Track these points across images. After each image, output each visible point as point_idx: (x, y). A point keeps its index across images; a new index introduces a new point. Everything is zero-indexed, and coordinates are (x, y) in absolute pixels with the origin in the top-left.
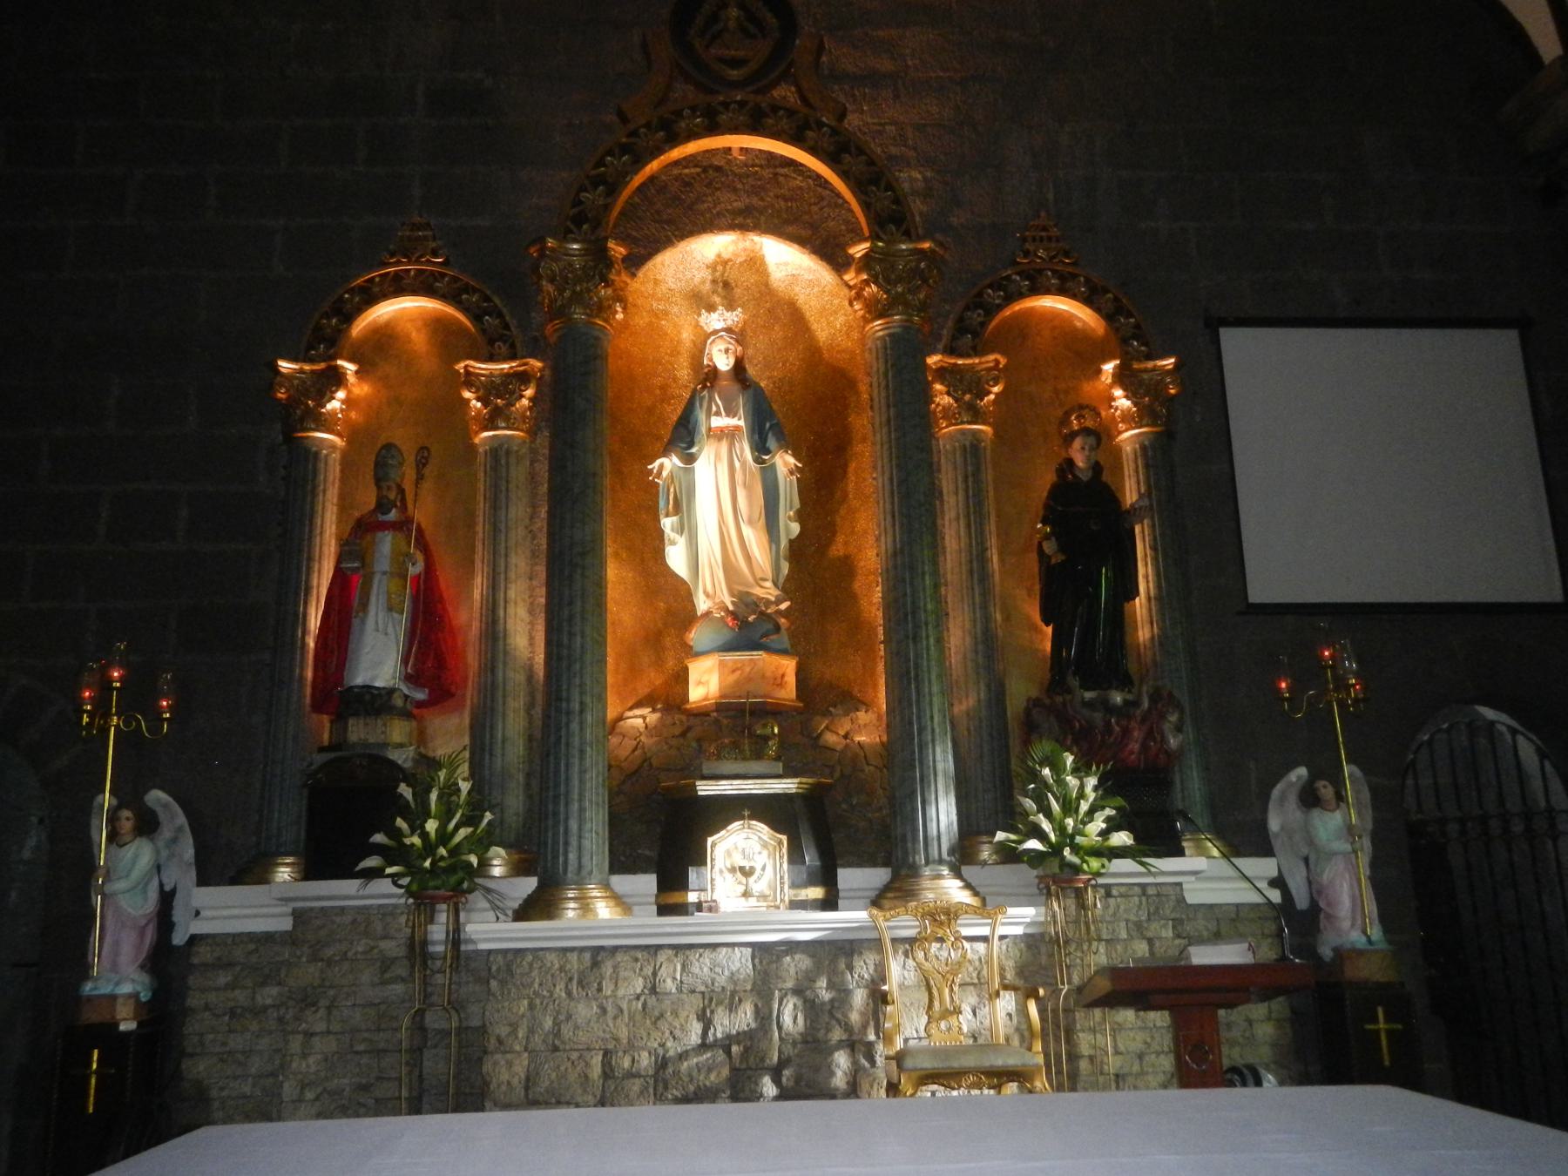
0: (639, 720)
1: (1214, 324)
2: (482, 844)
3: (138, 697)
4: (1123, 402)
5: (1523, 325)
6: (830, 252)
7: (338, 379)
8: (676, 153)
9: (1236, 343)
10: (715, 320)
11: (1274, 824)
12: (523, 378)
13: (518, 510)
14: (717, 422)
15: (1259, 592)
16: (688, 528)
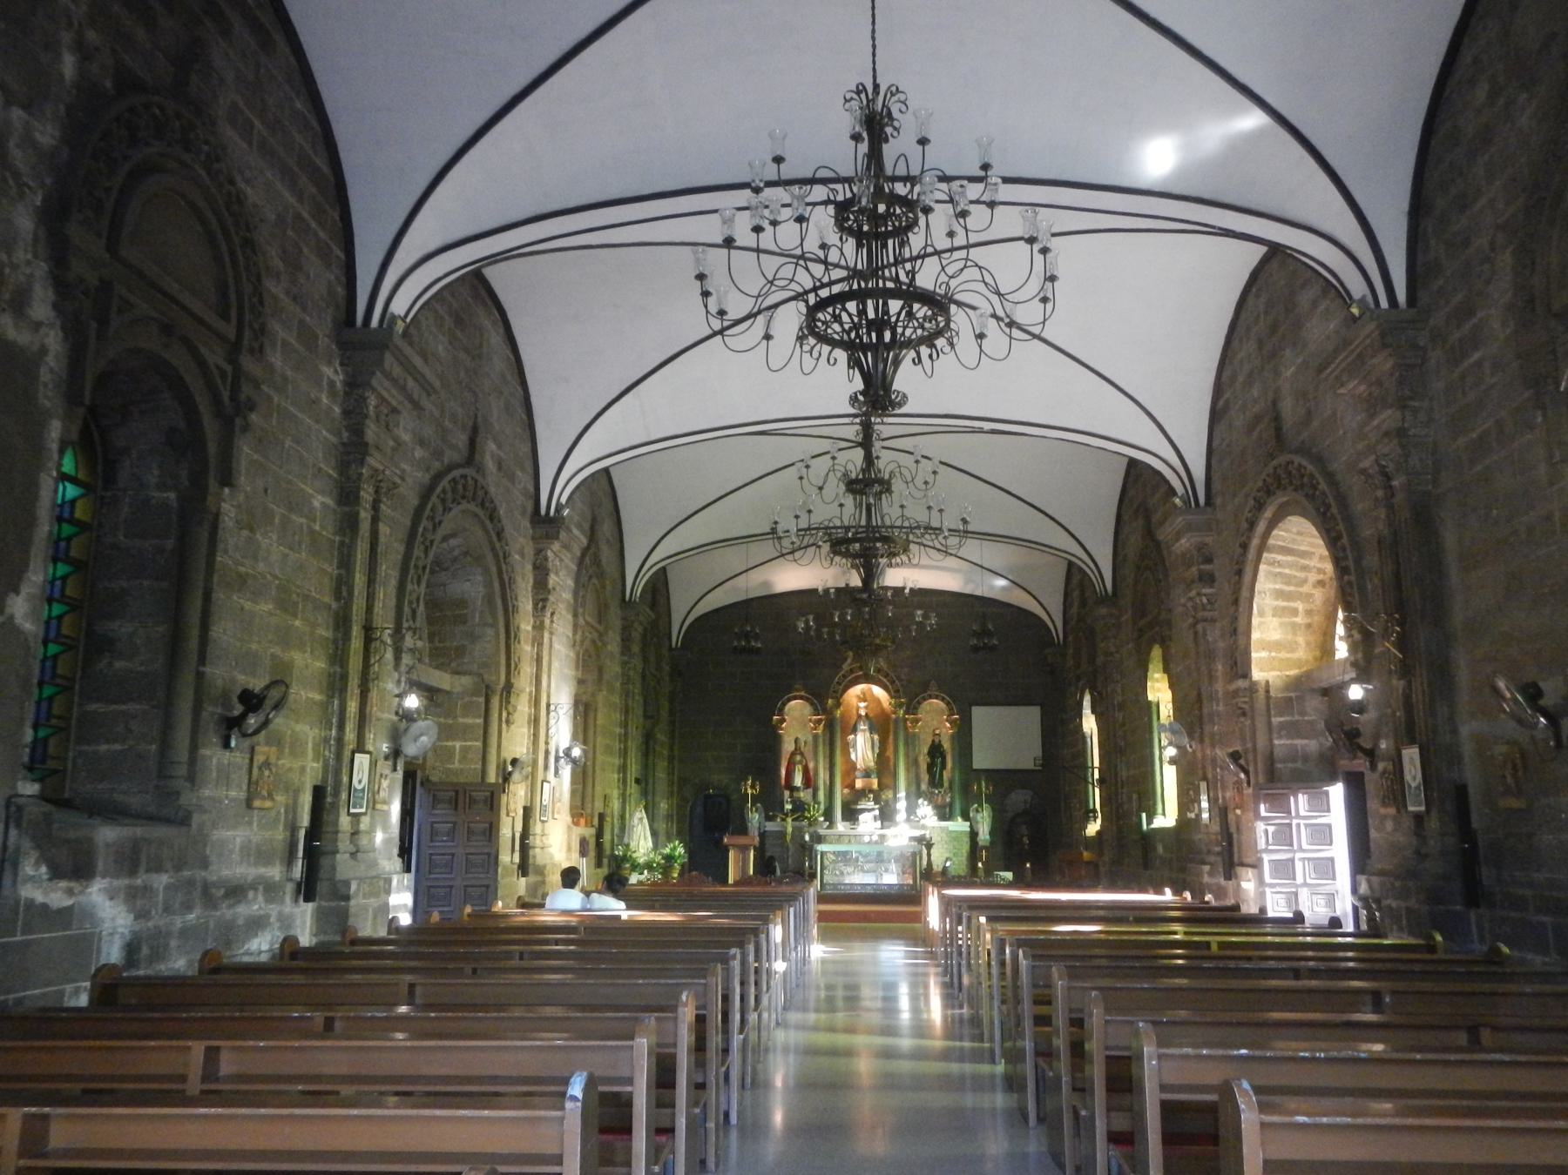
0: (846, 791)
1: (970, 706)
2: (819, 816)
3: (753, 787)
4: (948, 725)
5: (1042, 706)
6: (885, 688)
7: (783, 720)
8: (853, 675)
9: (978, 713)
10: (862, 705)
11: (971, 815)
12: (820, 720)
13: (821, 748)
14: (862, 727)
15: (974, 767)
16: (856, 751)
